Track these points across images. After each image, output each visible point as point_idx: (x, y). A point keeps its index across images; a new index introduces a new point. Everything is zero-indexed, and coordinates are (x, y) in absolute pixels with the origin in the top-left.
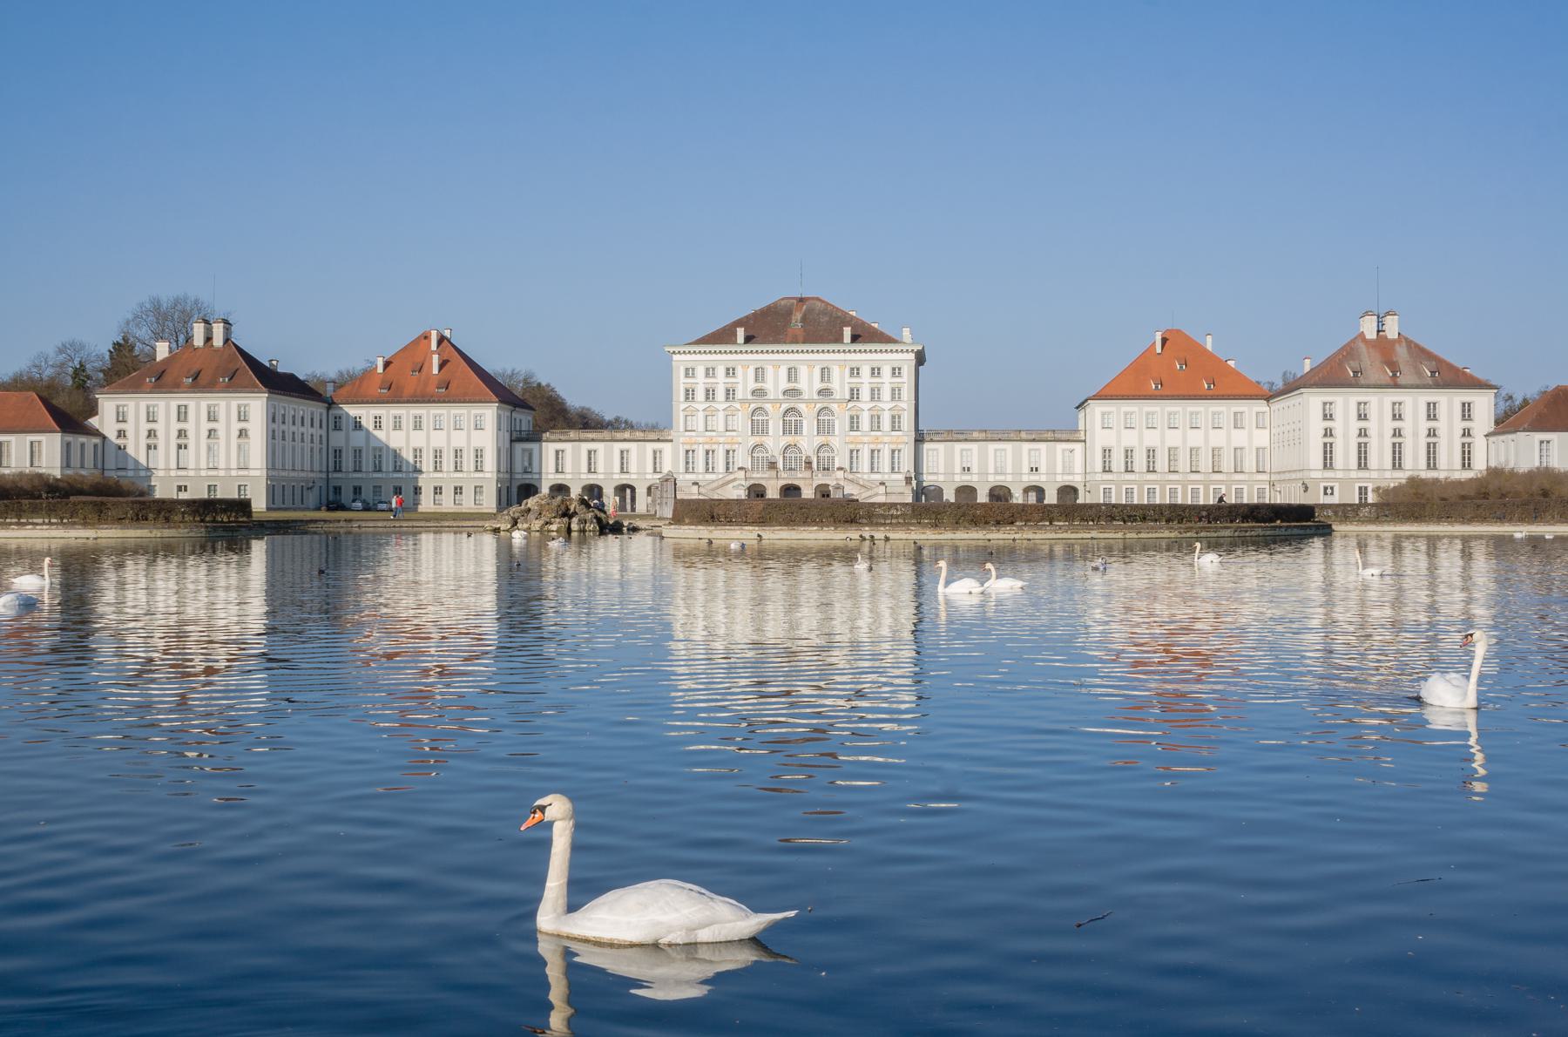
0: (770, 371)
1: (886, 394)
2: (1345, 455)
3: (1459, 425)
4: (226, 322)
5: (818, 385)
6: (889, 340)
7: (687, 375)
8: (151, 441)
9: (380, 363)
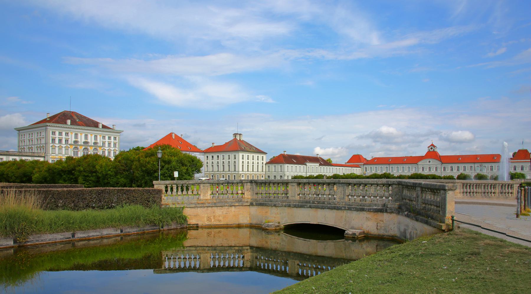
0: (79, 135)
2: (245, 169)
5: (93, 141)
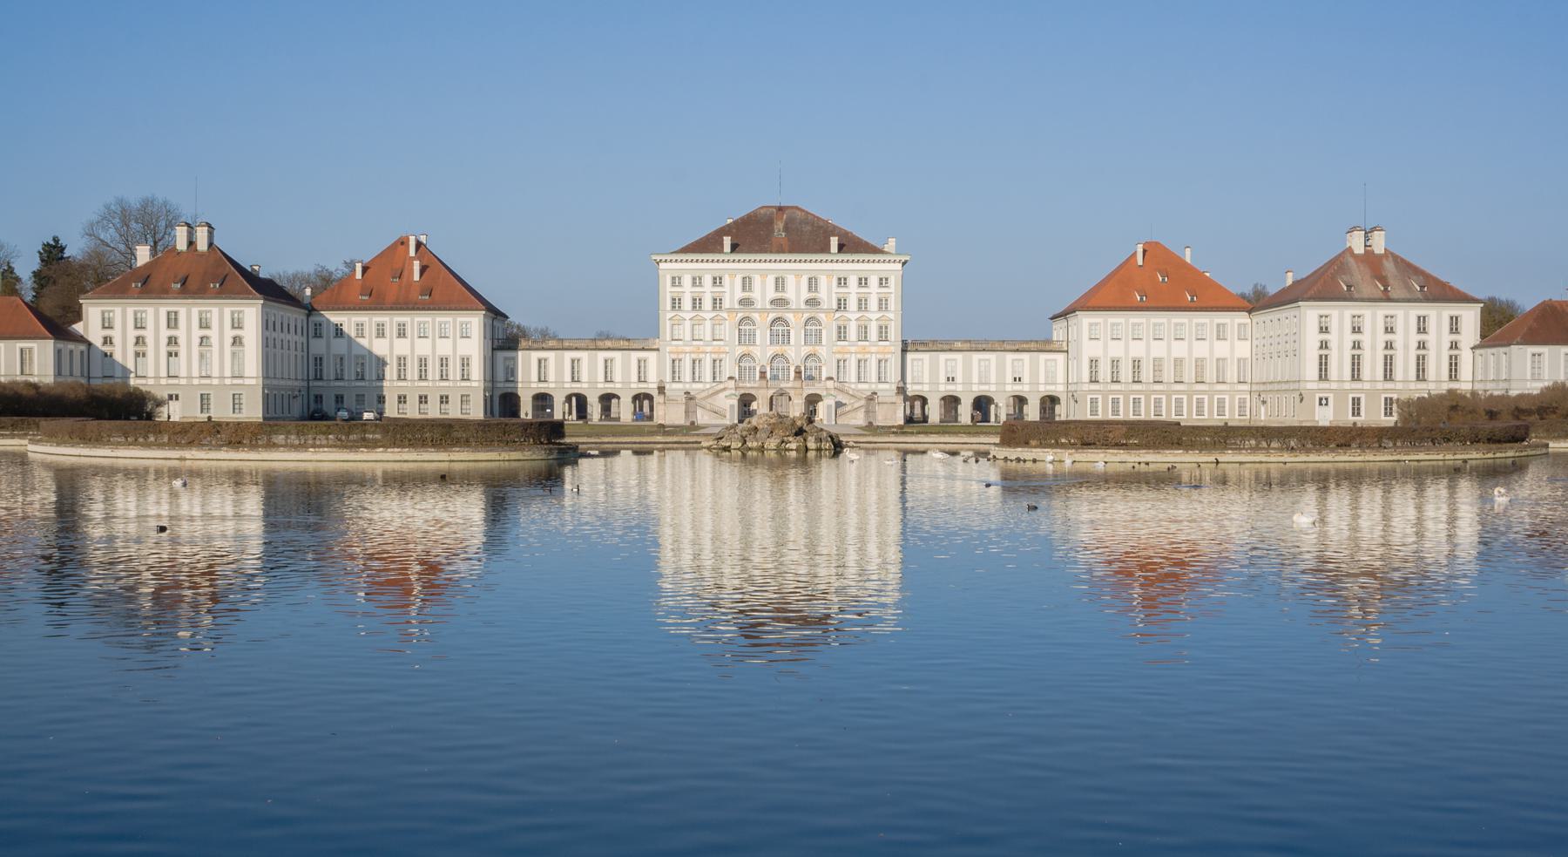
0: (757, 280)
1: (873, 304)
2: (1340, 367)
3: (1447, 338)
4: (209, 226)
5: (805, 295)
6: (881, 252)
7: (673, 284)
8: (139, 349)
9: (359, 268)
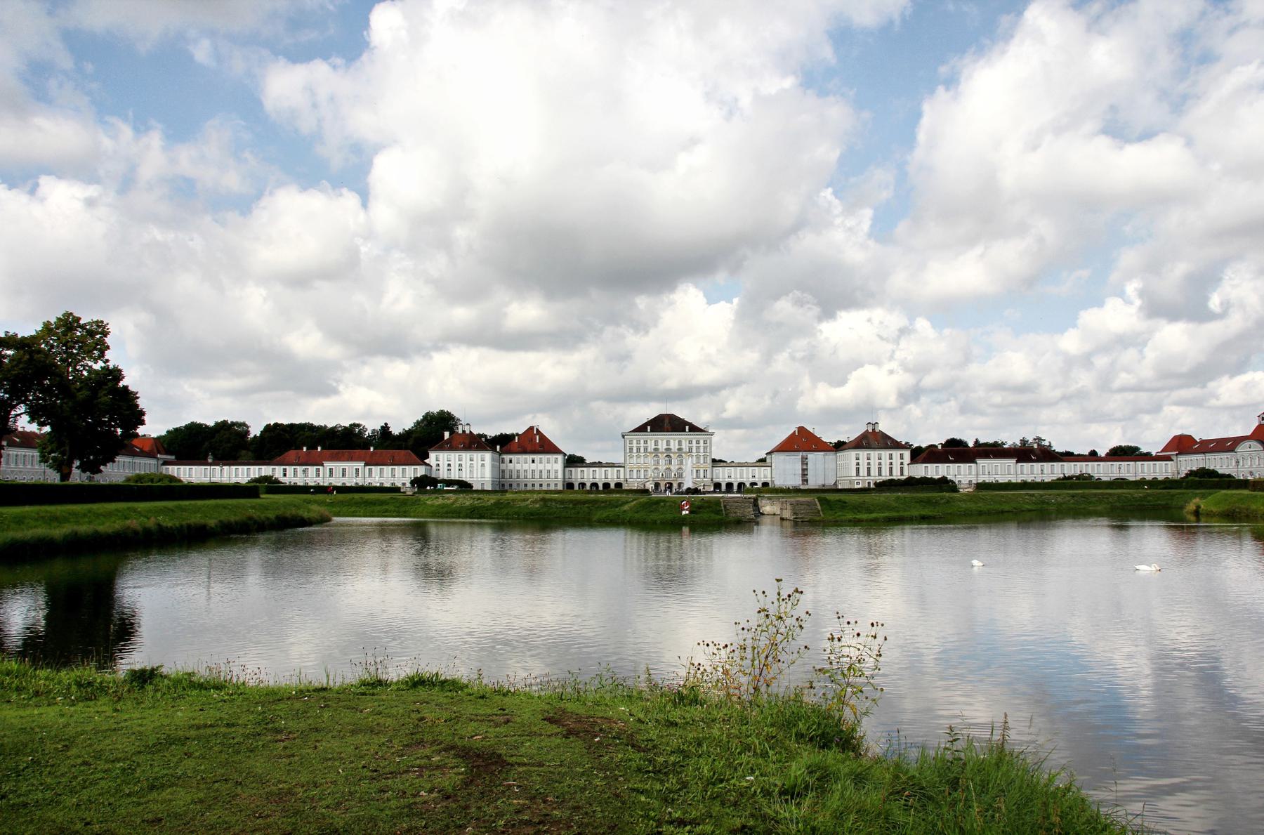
2: (863, 472)
